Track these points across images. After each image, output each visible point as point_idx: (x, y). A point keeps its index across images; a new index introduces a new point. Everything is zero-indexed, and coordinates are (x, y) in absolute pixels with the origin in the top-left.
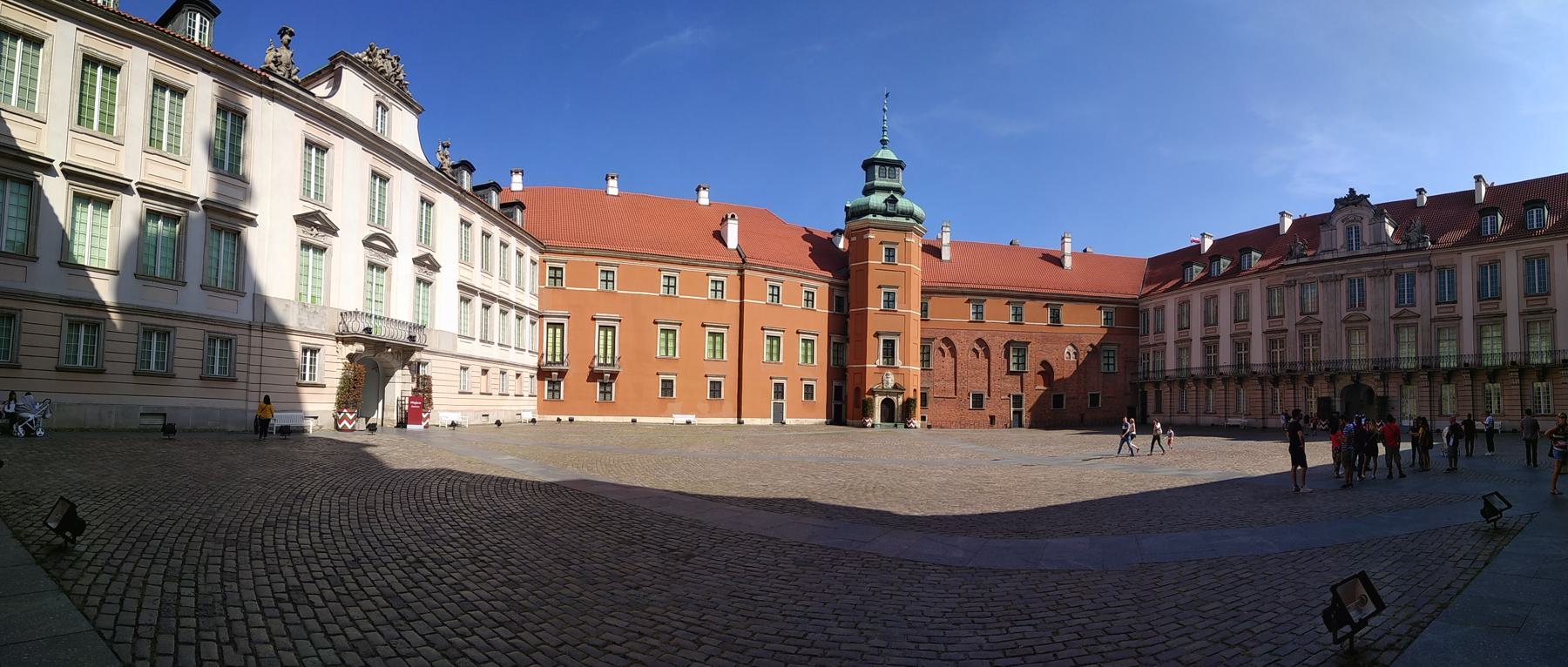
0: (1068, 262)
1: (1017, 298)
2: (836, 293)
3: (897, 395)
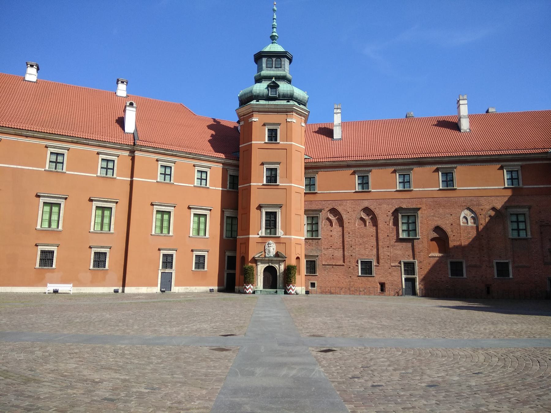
0: (465, 125)
1: (404, 166)
2: (231, 172)
3: (279, 262)
